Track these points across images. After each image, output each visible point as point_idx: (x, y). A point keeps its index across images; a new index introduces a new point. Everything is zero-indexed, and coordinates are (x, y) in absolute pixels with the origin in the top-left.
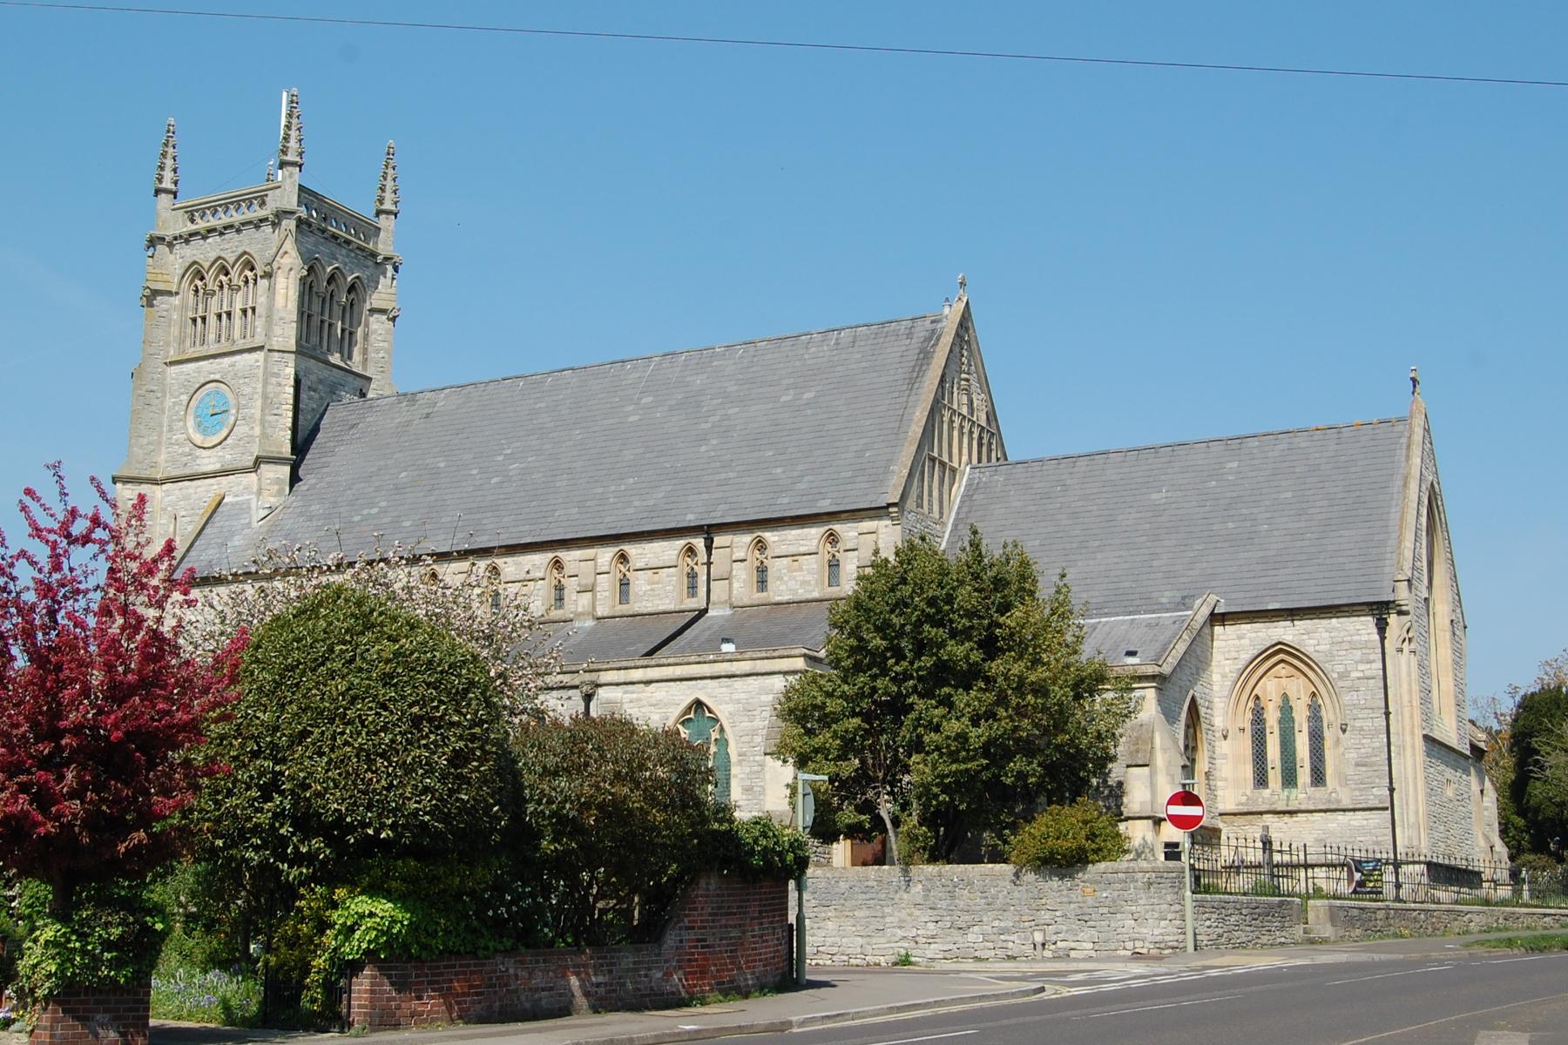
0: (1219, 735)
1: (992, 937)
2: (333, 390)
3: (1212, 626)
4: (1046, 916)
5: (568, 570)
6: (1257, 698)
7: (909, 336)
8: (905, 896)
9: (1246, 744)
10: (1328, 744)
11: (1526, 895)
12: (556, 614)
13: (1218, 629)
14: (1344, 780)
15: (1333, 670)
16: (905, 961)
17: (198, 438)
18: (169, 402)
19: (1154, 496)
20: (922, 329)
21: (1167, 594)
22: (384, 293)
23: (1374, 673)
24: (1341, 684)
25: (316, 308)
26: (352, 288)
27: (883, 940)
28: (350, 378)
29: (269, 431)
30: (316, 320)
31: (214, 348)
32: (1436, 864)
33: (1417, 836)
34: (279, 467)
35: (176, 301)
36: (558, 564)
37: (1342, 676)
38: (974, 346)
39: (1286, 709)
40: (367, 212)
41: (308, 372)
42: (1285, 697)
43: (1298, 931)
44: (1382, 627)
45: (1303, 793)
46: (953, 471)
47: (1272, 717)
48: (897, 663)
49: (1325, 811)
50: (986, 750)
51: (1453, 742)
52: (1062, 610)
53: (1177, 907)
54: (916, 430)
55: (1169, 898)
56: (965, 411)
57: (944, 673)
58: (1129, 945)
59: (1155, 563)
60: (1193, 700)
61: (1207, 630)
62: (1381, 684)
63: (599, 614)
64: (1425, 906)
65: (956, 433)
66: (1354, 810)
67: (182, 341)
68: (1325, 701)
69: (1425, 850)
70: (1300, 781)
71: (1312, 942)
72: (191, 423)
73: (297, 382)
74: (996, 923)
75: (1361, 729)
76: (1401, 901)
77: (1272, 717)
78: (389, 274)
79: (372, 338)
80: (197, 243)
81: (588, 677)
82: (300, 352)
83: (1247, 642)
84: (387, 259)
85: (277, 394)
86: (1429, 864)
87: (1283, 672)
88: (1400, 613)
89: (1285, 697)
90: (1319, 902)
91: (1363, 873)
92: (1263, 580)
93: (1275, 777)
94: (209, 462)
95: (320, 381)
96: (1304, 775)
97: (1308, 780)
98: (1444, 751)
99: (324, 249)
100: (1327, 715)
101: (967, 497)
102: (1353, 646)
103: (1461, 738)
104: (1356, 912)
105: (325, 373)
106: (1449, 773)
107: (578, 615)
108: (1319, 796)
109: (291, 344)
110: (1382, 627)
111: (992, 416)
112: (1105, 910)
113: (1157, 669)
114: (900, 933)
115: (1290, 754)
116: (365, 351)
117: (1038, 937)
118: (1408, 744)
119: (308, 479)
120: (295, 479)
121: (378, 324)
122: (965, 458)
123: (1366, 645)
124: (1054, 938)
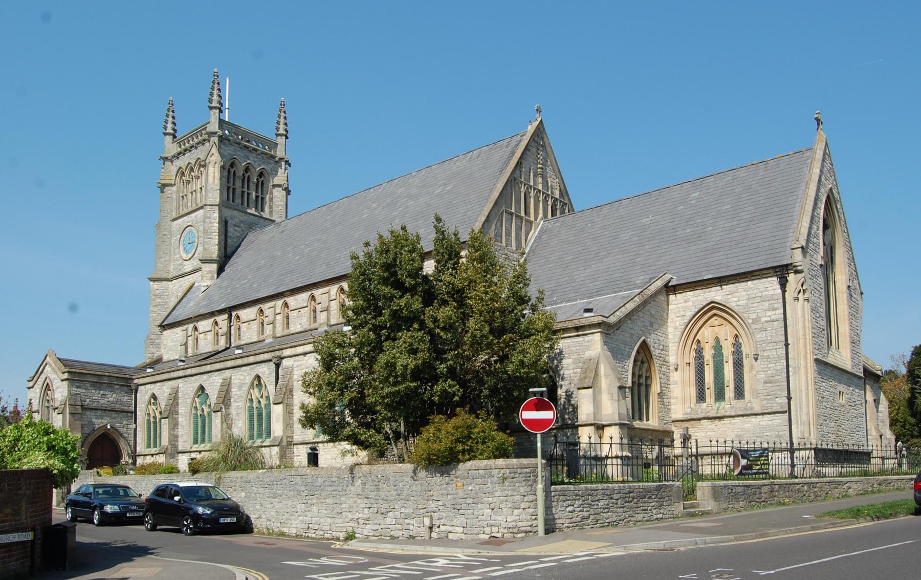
0: (672, 368)
1: (401, 521)
2: (251, 227)
3: (668, 295)
4: (433, 505)
5: (318, 299)
6: (699, 341)
7: (507, 146)
8: (352, 488)
9: (692, 373)
10: (746, 369)
11: (905, 467)
12: (314, 326)
13: (672, 297)
14: (756, 394)
15: (749, 317)
16: (350, 537)
17: (184, 256)
18: (174, 239)
19: (644, 220)
20: (513, 143)
21: (642, 278)
22: (280, 177)
23: (778, 317)
24: (754, 327)
25: (238, 184)
26: (261, 175)
27: (341, 521)
28: (262, 221)
29: (206, 247)
30: (238, 191)
31: (190, 209)
32: (820, 450)
33: (807, 430)
34: (211, 265)
35: (174, 188)
36: (313, 298)
37: (755, 321)
38: (548, 149)
39: (718, 347)
40: (270, 135)
41: (232, 217)
42: (717, 340)
43: (679, 508)
44: (783, 284)
45: (729, 405)
46: (531, 223)
47: (708, 354)
48: (375, 317)
49: (743, 416)
50: (416, 374)
51: (848, 365)
52: (521, 278)
53: (531, 498)
54: (496, 194)
55: (522, 490)
56: (540, 187)
57: (402, 321)
58: (488, 530)
59: (637, 260)
60: (644, 341)
61: (662, 298)
62: (783, 325)
63: (333, 322)
64: (808, 480)
65: (532, 200)
66: (763, 414)
67: (178, 208)
68: (743, 340)
69: (814, 439)
70: (727, 396)
71: (692, 515)
72: (181, 249)
73: (224, 224)
74: (403, 510)
75: (768, 357)
76: (796, 477)
77: (708, 354)
78: (283, 167)
79: (275, 200)
80: (182, 157)
81: (277, 353)
82: (223, 205)
83: (690, 304)
84: (281, 159)
85: (210, 228)
86: (816, 450)
87: (716, 323)
88: (797, 272)
89: (717, 340)
90: (705, 484)
91: (751, 461)
92: (704, 261)
93: (710, 394)
94: (188, 267)
95: (242, 222)
96: (730, 392)
97: (732, 395)
98: (836, 372)
99: (240, 155)
100: (745, 350)
101: (539, 237)
102: (763, 299)
103: (855, 365)
104: (740, 489)
105: (245, 218)
106: (841, 387)
107: (321, 324)
108: (739, 406)
109: (217, 201)
110: (783, 284)
111: (564, 192)
112: (470, 501)
113: (600, 319)
114: (350, 516)
115: (720, 379)
116: (271, 207)
117: (427, 522)
118: (803, 366)
119: (228, 269)
120: (221, 270)
121: (278, 194)
122: (541, 215)
123: (771, 298)
124: (438, 523)
